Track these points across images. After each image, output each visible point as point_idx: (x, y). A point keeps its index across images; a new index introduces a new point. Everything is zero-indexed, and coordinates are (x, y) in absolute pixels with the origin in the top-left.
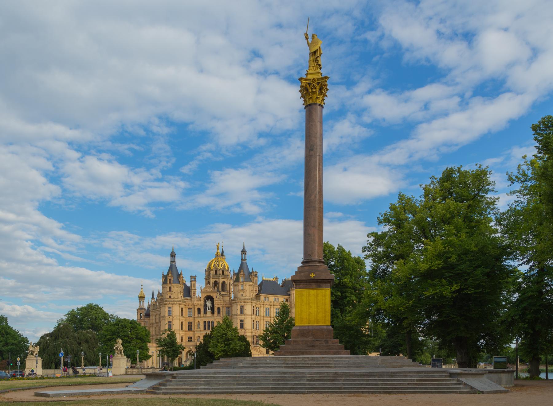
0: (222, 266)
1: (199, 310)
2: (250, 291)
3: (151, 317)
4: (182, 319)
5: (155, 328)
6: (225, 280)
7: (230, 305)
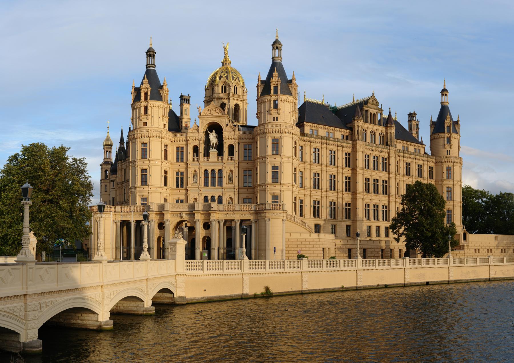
0: (233, 79)
1: (196, 149)
2: (290, 113)
3: (119, 173)
4: (166, 165)
5: (125, 190)
6: (240, 103)
7: (251, 141)
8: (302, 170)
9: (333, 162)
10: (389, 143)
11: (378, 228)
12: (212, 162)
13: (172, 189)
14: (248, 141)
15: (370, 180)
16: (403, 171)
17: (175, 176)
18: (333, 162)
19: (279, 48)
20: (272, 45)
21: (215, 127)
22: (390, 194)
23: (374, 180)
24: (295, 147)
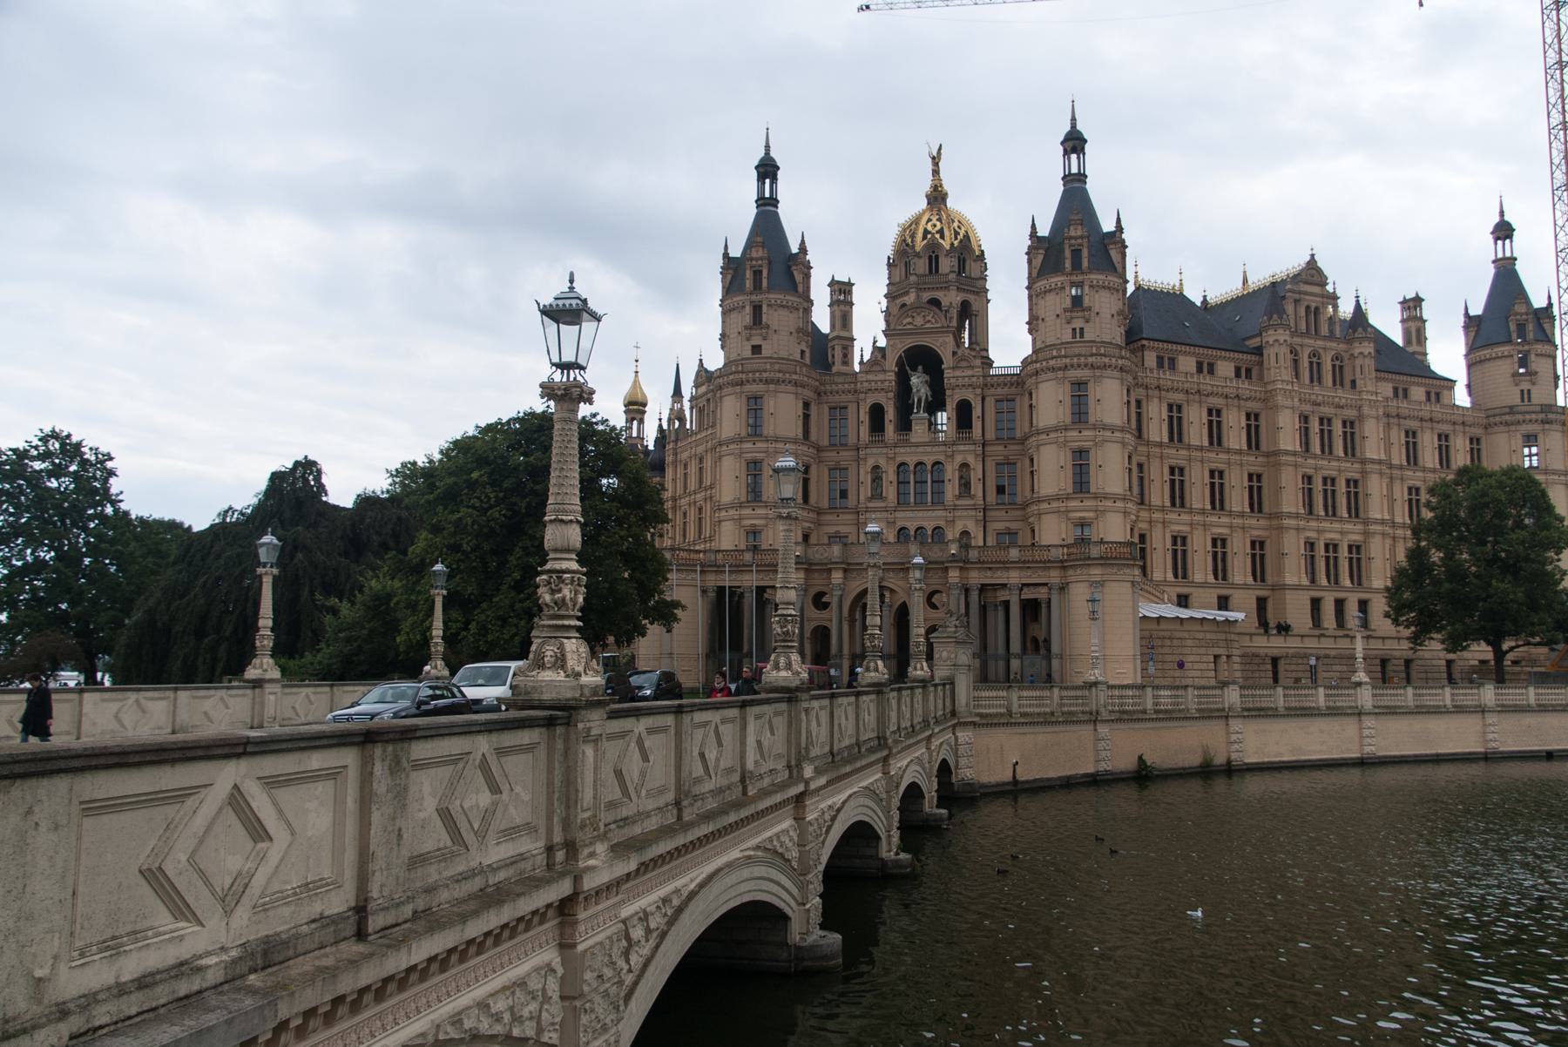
0: (956, 239)
1: (877, 413)
2: (1113, 316)
3: (669, 473)
5: (685, 514)
6: (971, 298)
7: (1013, 390)
8: (1143, 459)
9: (1215, 435)
10: (1358, 382)
11: (1340, 604)
12: (917, 445)
13: (819, 512)
14: (1006, 391)
15: (1314, 479)
16: (1398, 457)
17: (826, 479)
18: (1215, 435)
19: (1079, 148)
20: (1062, 143)
21: (922, 359)
22: (1366, 511)
23: (1325, 479)
24: (1129, 402)
